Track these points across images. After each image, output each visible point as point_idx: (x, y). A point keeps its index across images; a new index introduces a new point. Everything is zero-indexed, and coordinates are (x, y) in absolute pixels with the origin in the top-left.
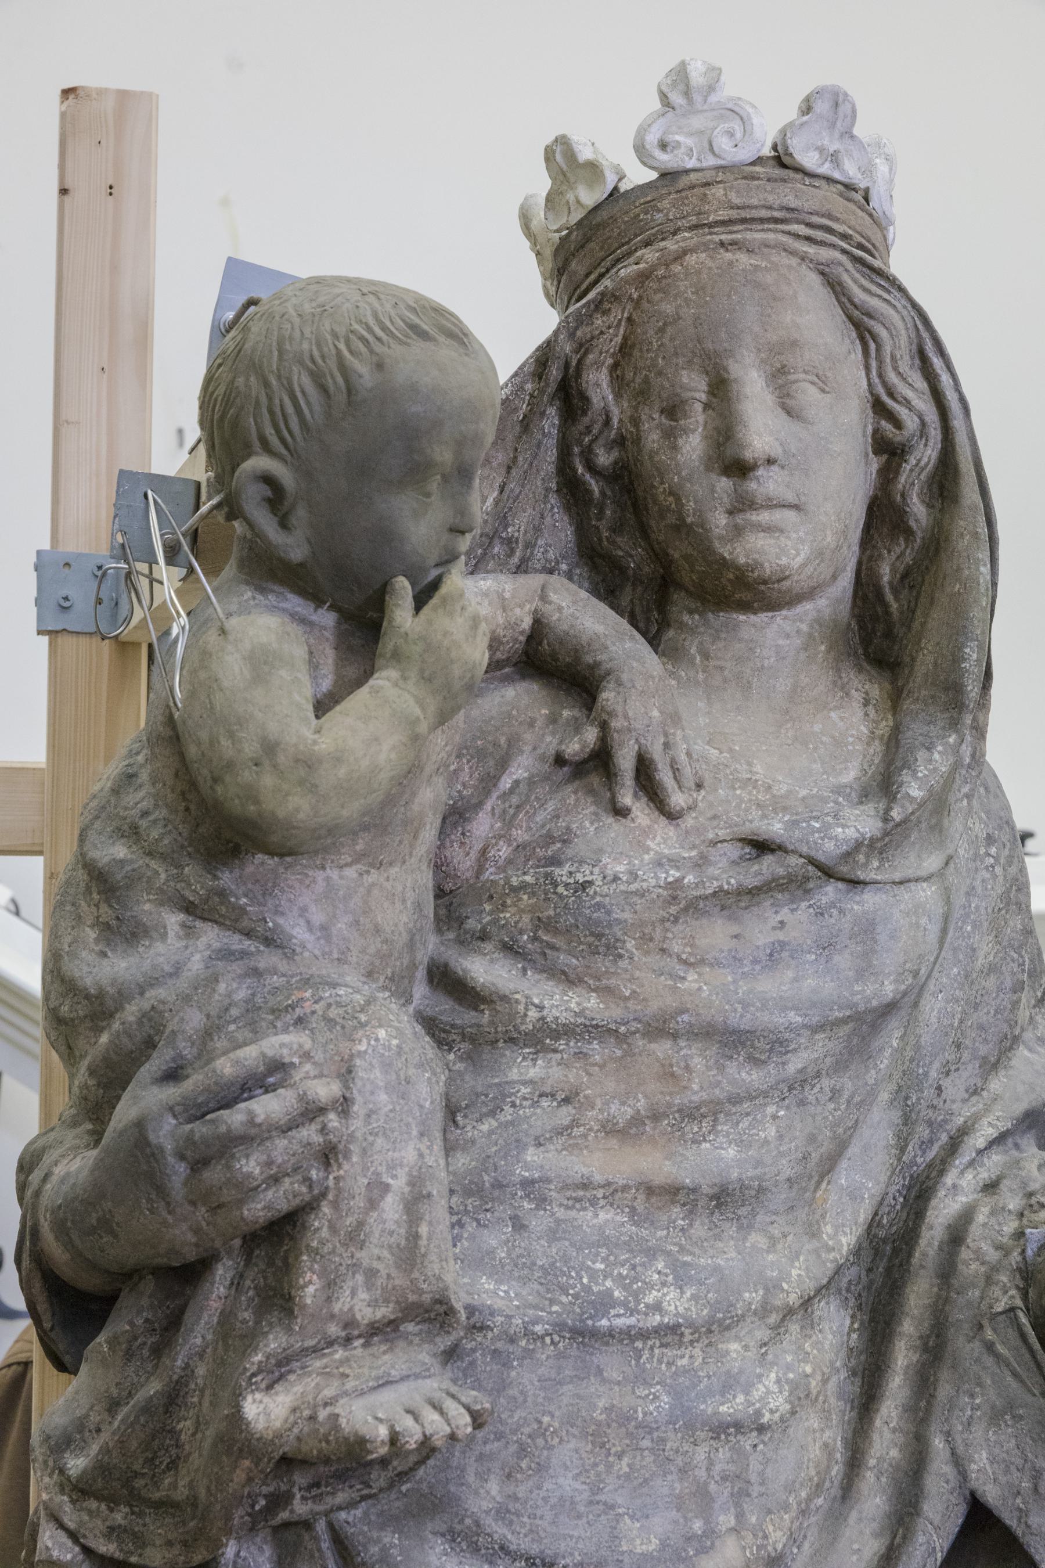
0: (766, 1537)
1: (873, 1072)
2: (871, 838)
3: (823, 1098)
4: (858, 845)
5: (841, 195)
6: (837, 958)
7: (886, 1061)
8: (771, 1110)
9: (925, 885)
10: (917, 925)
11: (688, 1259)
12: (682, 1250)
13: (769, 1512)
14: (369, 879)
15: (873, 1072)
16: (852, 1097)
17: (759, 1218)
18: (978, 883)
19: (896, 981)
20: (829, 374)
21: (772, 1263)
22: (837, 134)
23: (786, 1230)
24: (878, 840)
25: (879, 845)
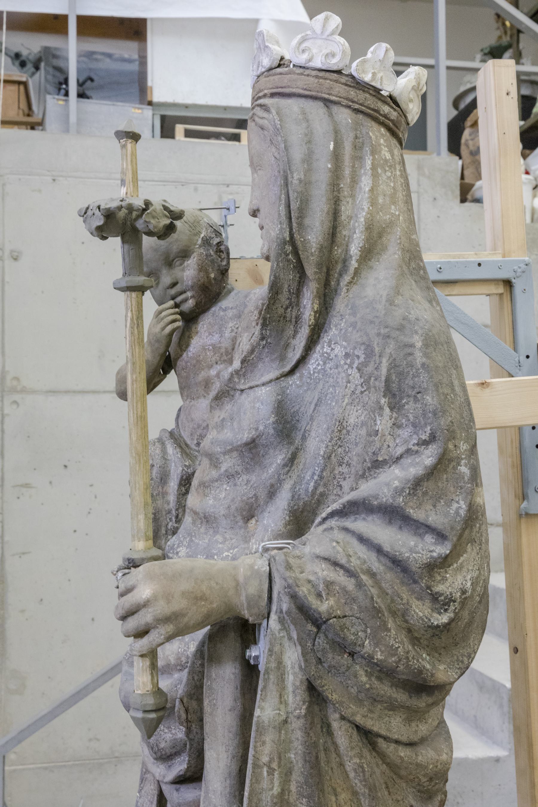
0: (188, 648)
1: (265, 474)
2: (235, 371)
3: (243, 483)
4: (232, 374)
5: (265, 77)
6: (234, 424)
7: (272, 469)
8: (225, 486)
9: (263, 388)
10: (254, 407)
11: (193, 539)
12: (195, 536)
13: (194, 640)
14: (191, 404)
15: (265, 474)
16: (253, 484)
17: (220, 529)
18: (339, 380)
19: (248, 433)
20: (261, 163)
21: (219, 548)
22: (263, 51)
23: (232, 536)
24: (239, 371)
25: (241, 373)
